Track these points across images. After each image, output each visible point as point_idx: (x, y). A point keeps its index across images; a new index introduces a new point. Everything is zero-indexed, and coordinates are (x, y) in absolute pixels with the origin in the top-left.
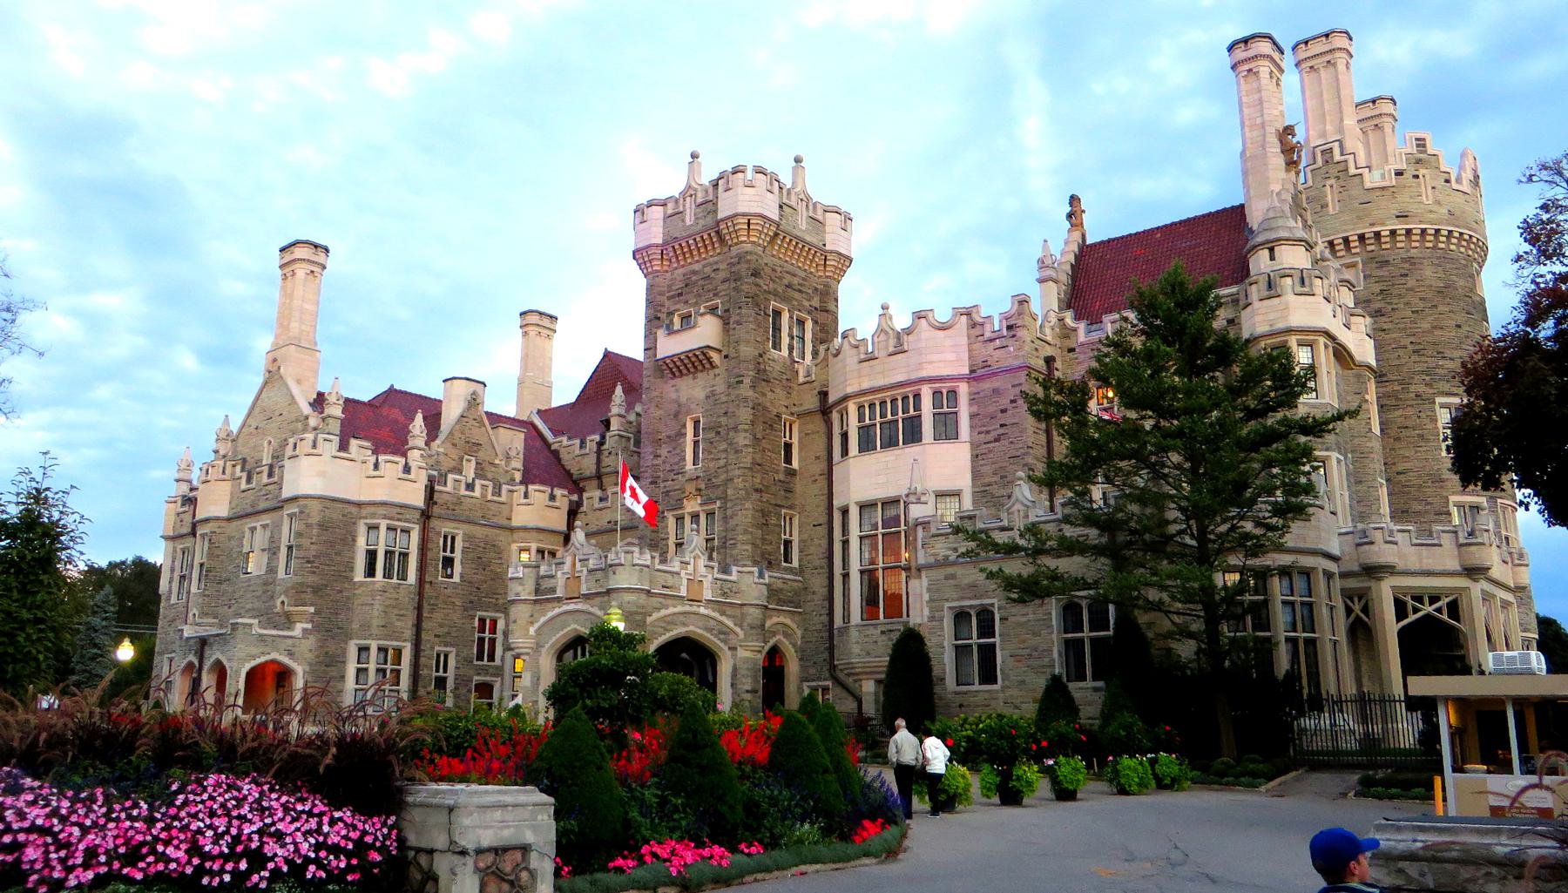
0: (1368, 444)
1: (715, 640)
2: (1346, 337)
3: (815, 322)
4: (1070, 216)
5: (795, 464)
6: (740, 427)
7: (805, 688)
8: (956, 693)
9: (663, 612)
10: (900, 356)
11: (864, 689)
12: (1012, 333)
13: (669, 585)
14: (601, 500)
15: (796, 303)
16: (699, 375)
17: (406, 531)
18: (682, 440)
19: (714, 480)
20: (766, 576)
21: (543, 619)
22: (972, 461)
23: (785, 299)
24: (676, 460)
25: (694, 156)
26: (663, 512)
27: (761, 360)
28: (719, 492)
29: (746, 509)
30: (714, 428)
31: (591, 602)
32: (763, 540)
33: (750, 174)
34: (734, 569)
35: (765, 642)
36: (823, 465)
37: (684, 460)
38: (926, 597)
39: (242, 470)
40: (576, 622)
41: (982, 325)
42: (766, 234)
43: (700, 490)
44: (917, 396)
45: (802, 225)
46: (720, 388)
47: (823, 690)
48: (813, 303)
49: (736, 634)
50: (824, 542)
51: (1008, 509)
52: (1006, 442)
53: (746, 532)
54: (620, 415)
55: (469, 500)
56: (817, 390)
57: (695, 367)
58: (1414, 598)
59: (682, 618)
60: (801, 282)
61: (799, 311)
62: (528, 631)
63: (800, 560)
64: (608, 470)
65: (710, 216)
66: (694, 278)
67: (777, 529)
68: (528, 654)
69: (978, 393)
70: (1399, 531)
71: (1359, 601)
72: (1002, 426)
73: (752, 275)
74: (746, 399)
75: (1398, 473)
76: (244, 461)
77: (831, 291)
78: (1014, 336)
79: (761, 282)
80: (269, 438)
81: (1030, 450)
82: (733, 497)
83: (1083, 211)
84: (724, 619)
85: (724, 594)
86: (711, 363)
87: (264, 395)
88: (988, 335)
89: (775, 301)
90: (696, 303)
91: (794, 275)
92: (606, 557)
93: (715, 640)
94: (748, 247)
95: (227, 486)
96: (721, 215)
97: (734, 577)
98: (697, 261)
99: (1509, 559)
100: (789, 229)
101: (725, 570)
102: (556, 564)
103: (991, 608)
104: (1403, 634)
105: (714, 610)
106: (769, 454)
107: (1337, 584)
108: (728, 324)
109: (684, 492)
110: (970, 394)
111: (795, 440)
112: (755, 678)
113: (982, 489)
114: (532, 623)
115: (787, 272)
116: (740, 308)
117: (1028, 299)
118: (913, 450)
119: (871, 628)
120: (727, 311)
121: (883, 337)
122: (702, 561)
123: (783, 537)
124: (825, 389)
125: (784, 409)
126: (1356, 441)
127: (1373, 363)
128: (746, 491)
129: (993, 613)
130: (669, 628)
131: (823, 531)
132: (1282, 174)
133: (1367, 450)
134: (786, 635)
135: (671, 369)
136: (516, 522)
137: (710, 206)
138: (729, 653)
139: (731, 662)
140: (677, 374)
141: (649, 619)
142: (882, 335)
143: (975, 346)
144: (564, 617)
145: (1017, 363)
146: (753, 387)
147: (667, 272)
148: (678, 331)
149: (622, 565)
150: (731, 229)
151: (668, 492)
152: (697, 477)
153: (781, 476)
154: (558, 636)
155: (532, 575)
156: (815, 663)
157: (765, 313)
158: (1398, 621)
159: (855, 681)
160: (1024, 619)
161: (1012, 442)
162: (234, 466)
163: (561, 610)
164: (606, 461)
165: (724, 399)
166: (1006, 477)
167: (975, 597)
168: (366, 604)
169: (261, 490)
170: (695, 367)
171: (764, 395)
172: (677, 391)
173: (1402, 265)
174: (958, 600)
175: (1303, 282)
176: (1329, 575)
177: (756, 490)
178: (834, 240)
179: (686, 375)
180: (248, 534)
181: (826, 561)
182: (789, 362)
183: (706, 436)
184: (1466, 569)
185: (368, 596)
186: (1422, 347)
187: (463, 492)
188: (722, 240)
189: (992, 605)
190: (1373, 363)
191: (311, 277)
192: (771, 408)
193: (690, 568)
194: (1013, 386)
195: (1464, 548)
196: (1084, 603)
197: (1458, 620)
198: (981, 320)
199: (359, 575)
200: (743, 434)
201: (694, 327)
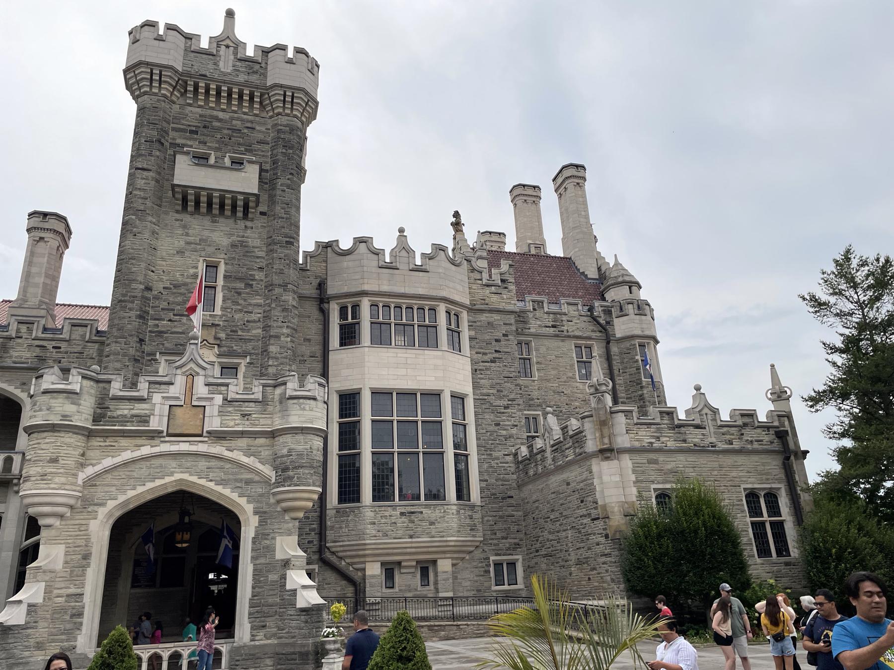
6: (290, 286)
10: (421, 274)
11: (367, 574)
16: (221, 220)
19: (240, 333)
21: (108, 462)
24: (180, 299)
25: (230, 14)
28: (249, 347)
36: (317, 349)
38: (633, 478)
40: (188, 470)
44: (433, 310)
51: (700, 411)
52: (501, 365)
62: (75, 475)
66: (216, 124)
68: (61, 516)
69: (475, 322)
72: (496, 351)
78: (506, 288)
82: (278, 355)
90: (217, 150)
98: (223, 110)
102: (150, 383)
110: (469, 322)
113: (481, 397)
114: (82, 466)
118: (429, 353)
121: (404, 253)
135: (185, 200)
137: (257, 67)
140: (191, 208)
143: (474, 287)
144: (157, 462)
147: (174, 103)
148: (211, 166)
149: (315, 399)
154: (140, 489)
155: (93, 391)
163: (156, 450)
165: (262, 254)
166: (502, 392)
174: (662, 483)
179: (203, 215)
194: (504, 324)
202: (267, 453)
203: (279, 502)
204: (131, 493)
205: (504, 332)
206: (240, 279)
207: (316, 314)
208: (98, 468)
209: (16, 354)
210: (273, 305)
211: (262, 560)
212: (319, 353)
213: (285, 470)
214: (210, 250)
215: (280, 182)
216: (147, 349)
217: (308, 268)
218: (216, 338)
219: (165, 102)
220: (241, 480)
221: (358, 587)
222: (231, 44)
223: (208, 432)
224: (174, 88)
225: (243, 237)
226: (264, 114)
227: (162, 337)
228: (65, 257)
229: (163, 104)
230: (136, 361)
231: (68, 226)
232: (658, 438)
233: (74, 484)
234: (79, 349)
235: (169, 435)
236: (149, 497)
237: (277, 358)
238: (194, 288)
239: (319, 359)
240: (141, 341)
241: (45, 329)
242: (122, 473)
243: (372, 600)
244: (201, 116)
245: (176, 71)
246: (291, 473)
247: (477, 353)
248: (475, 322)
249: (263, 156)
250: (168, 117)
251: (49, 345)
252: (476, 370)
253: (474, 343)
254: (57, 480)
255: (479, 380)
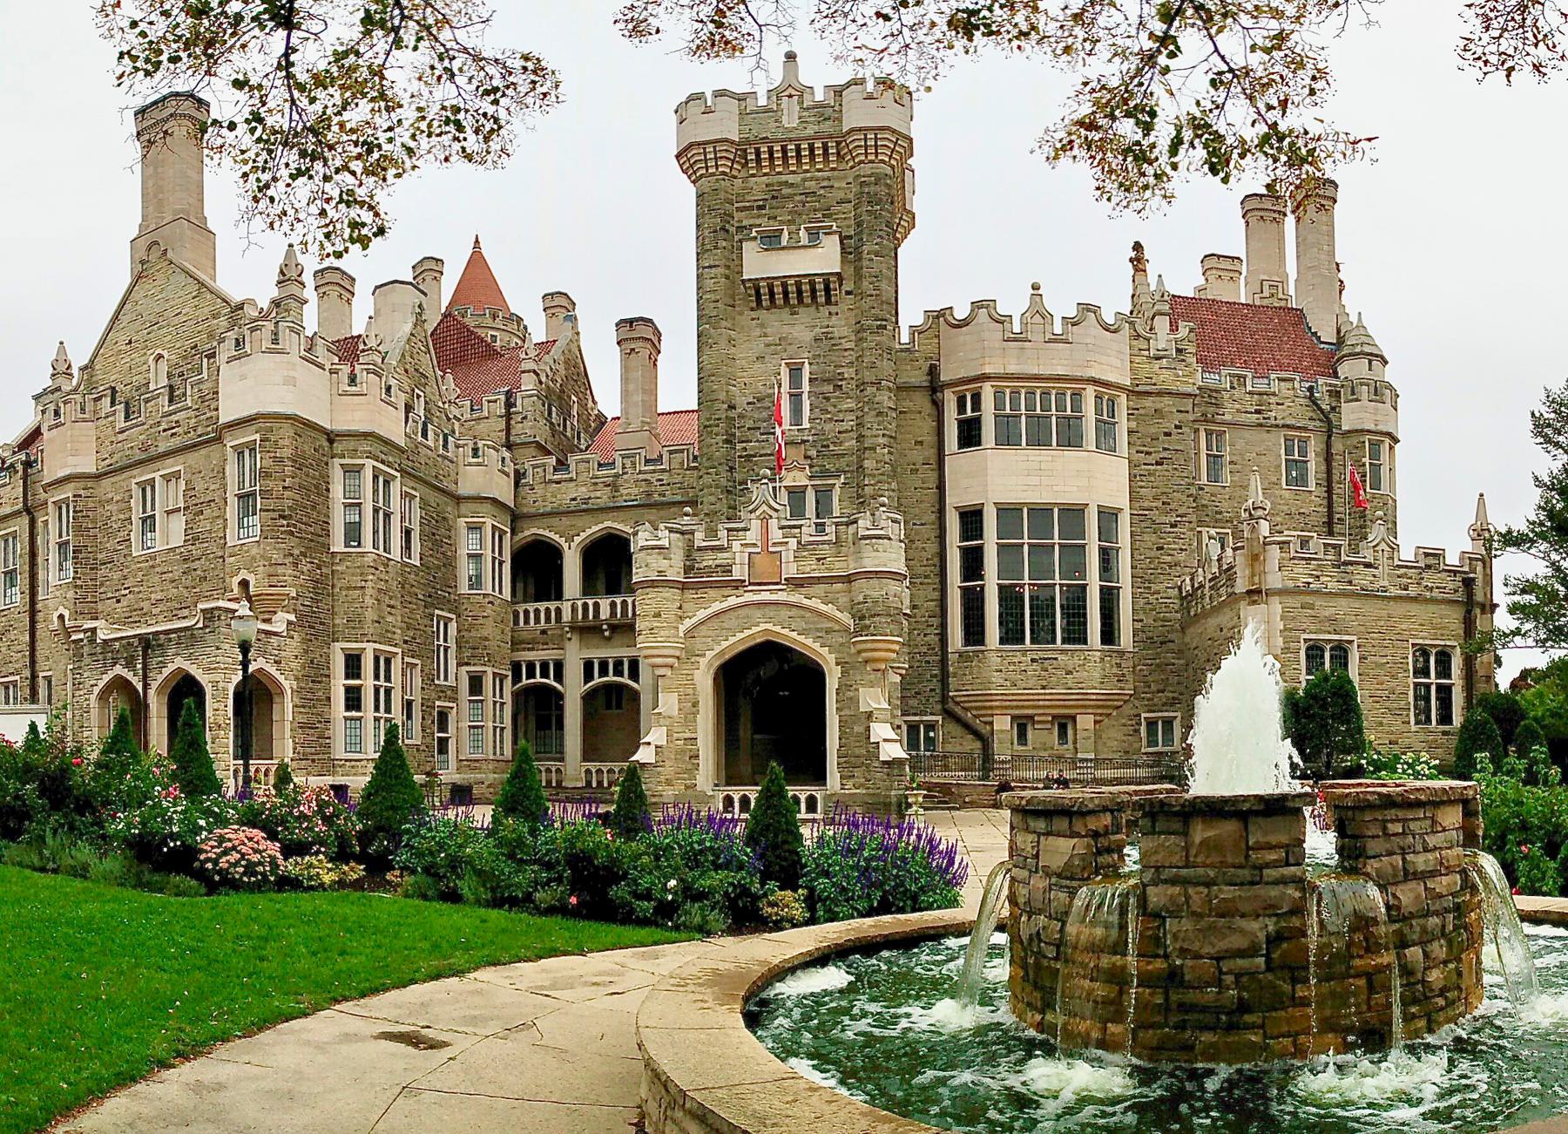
14: (555, 470)
17: (386, 483)
28: (843, 463)
54: (534, 372)
55: (423, 451)
64: (523, 439)
136: (463, 490)
152: (804, 442)
154: (732, 640)
164: (517, 428)
168: (355, 588)
185: (353, 575)
187: (420, 439)
199: (338, 545)
202: (845, 599)
203: (859, 652)
204: (725, 644)
208: (694, 620)
209: (626, 492)
210: (866, 410)
213: (862, 618)
224: (733, 161)
228: (658, 363)
231: (656, 328)
233: (677, 636)
234: (679, 479)
236: (741, 648)
237: (874, 476)
241: (647, 461)
242: (715, 623)
246: (867, 622)
251: (653, 478)
254: (662, 633)
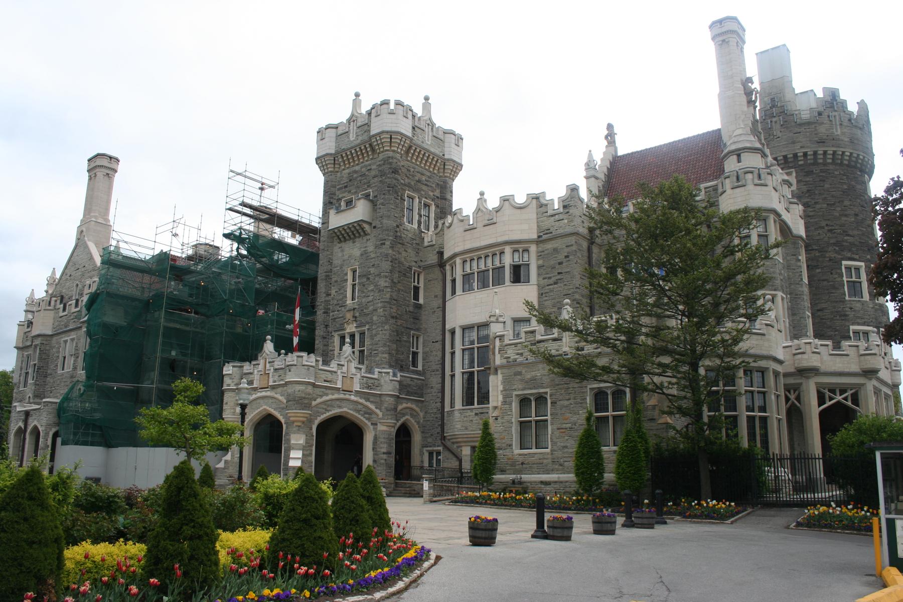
0: (800, 289)
1: (362, 418)
2: (786, 216)
3: (437, 206)
4: (606, 137)
5: (421, 301)
6: (382, 274)
7: (425, 451)
8: (520, 455)
9: (325, 398)
11: (464, 453)
12: (567, 210)
13: (329, 379)
15: (423, 193)
16: (357, 240)
18: (345, 284)
19: (365, 311)
20: (399, 375)
22: (539, 298)
23: (417, 190)
24: (341, 297)
26: (331, 333)
27: (398, 229)
28: (368, 319)
29: (386, 330)
30: (366, 276)
31: (275, 390)
32: (397, 350)
33: (392, 106)
34: (377, 370)
35: (398, 421)
36: (440, 301)
37: (346, 297)
38: (501, 388)
39: (61, 302)
41: (546, 205)
42: (403, 146)
43: (356, 317)
44: (502, 253)
45: (427, 142)
46: (371, 248)
47: (437, 453)
48: (435, 193)
49: (378, 415)
50: (440, 354)
52: (562, 285)
53: (385, 345)
56: (437, 250)
57: (354, 235)
58: (830, 391)
59: (338, 403)
60: (427, 179)
61: (426, 198)
63: (423, 366)
65: (366, 134)
66: (355, 176)
67: (407, 344)
69: (543, 251)
70: (822, 345)
71: (794, 393)
72: (559, 273)
73: (392, 172)
74: (387, 256)
75: (818, 310)
76: (62, 298)
77: (448, 186)
78: (568, 212)
79: (399, 178)
80: (77, 282)
81: (578, 290)
82: (377, 322)
83: (616, 134)
84: (368, 404)
85: (368, 387)
86: (364, 232)
87: (75, 254)
88: (550, 212)
89: (409, 191)
90: (356, 192)
91: (423, 174)
92: (285, 360)
93: (362, 418)
94: (391, 154)
95: (51, 314)
96: (373, 132)
97: (376, 376)
98: (358, 164)
99: (888, 366)
100: (419, 143)
101: (370, 370)
103: (545, 396)
104: (822, 414)
105: (361, 398)
106: (403, 293)
107: (782, 380)
108: (376, 205)
109: (344, 319)
110: (538, 252)
111: (421, 285)
112: (390, 445)
115: (418, 172)
116: (384, 194)
117: (577, 187)
118: (498, 289)
119: (469, 411)
120: (376, 197)
122: (354, 364)
123: (411, 349)
124: (442, 250)
125: (414, 263)
126: (792, 286)
127: (804, 235)
128: (386, 317)
129: (546, 399)
130: (328, 409)
131: (438, 346)
132: (745, 108)
133: (799, 293)
134: (412, 416)
135: (338, 236)
137: (366, 128)
138: (372, 427)
139: (373, 434)
140: (342, 239)
141: (314, 403)
142: (480, 214)
145: (569, 230)
146: (392, 247)
147: (337, 172)
148: (343, 211)
150: (379, 142)
151: (335, 319)
152: (354, 309)
153: (411, 309)
154: (254, 413)
156: (431, 435)
157: (401, 198)
158: (819, 407)
159: (458, 447)
160: (566, 403)
161: (565, 285)
162: (56, 301)
165: (373, 255)
167: (535, 388)
169: (70, 316)
170: (354, 235)
171: (400, 253)
172: (342, 251)
173: (821, 174)
175: (759, 177)
176: (776, 374)
177: (393, 317)
178: (451, 153)
180: (62, 345)
181: (440, 366)
182: (417, 232)
183: (360, 281)
184: (863, 371)
186: (833, 228)
188: (373, 150)
189: (546, 393)
190: (804, 235)
191: (106, 178)
192: (405, 263)
193: (345, 369)
195: (862, 358)
196: (609, 392)
197: (858, 406)
198: (545, 202)
200: (385, 279)
201: (354, 207)
205: (566, 254)
206: (364, 276)
207: (440, 276)
211: (286, 445)
212: (441, 306)
214: (353, 261)
215: (378, 203)
216: (330, 329)
217: (434, 243)
218: (355, 317)
219: (331, 175)
220: (280, 408)
221: (460, 461)
222: (355, 119)
223: (270, 386)
225: (366, 247)
226: (376, 156)
227: (334, 321)
229: (330, 177)
230: (324, 338)
232: (521, 354)
235: (260, 389)
237: (376, 324)
238: (346, 288)
239: (441, 309)
240: (327, 326)
243: (466, 471)
244: (349, 174)
245: (331, 154)
247: (544, 279)
248: (543, 251)
249: (375, 186)
250: (333, 183)
252: (542, 294)
253: (542, 271)
255: (544, 303)
